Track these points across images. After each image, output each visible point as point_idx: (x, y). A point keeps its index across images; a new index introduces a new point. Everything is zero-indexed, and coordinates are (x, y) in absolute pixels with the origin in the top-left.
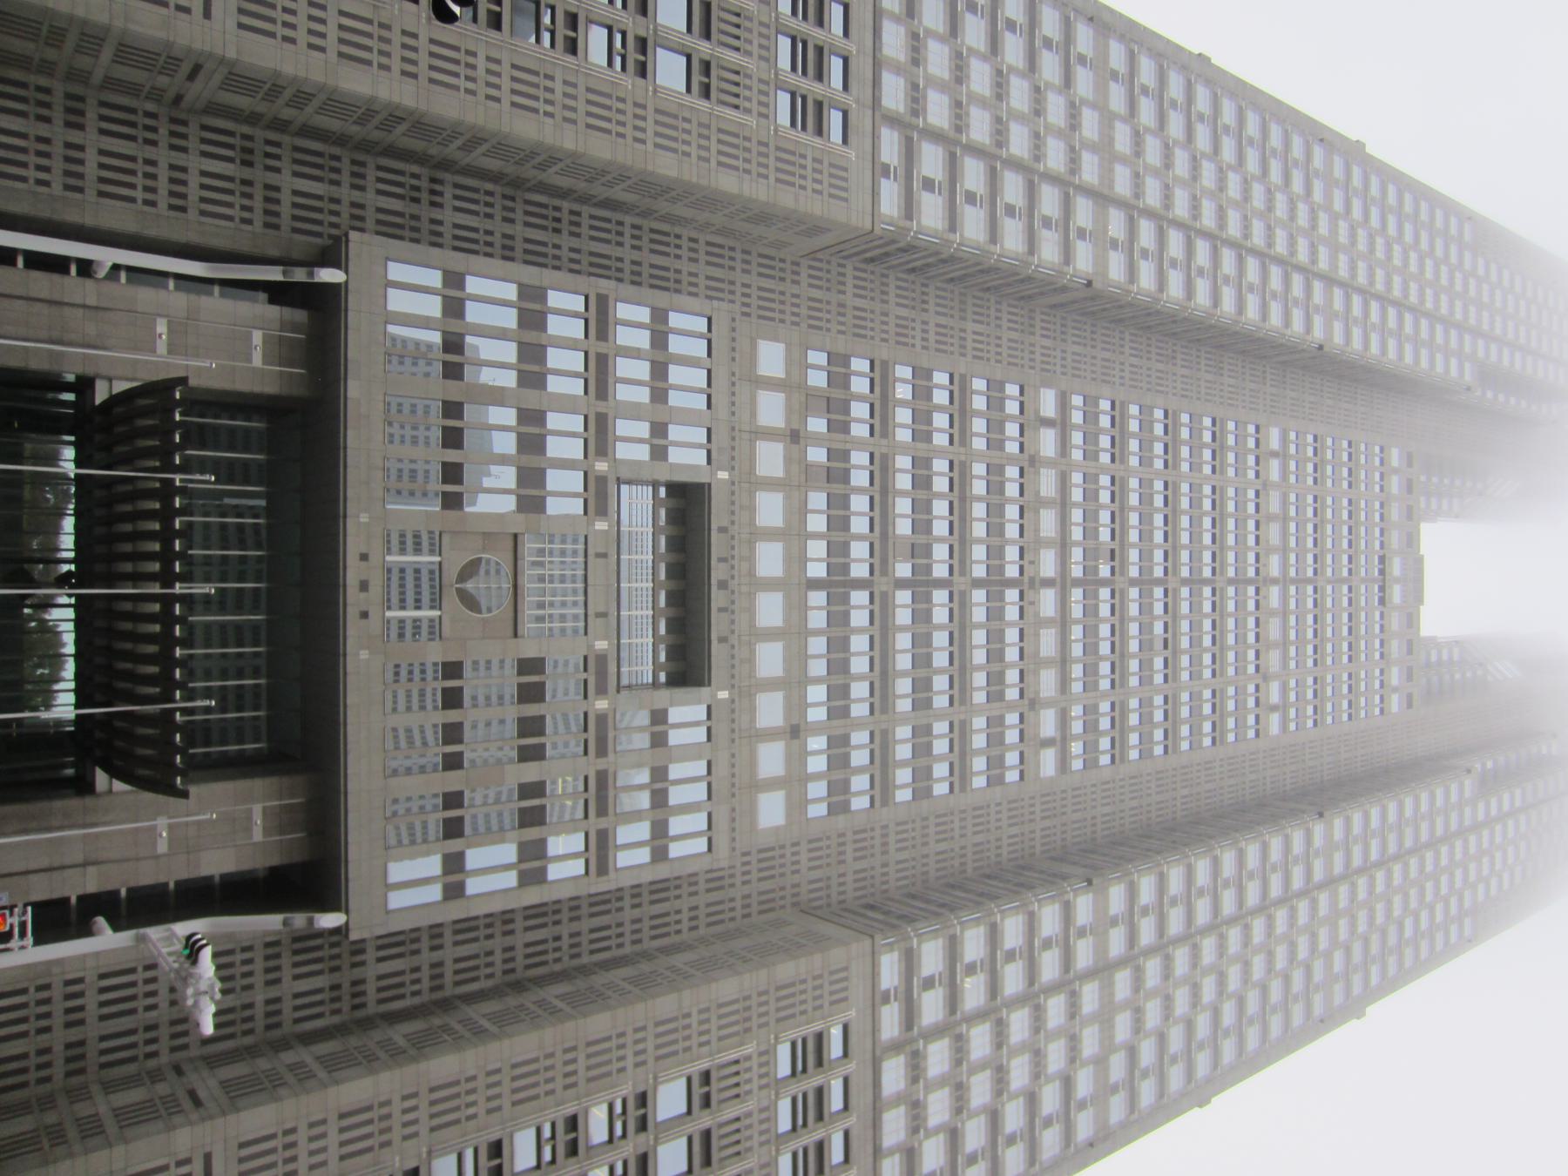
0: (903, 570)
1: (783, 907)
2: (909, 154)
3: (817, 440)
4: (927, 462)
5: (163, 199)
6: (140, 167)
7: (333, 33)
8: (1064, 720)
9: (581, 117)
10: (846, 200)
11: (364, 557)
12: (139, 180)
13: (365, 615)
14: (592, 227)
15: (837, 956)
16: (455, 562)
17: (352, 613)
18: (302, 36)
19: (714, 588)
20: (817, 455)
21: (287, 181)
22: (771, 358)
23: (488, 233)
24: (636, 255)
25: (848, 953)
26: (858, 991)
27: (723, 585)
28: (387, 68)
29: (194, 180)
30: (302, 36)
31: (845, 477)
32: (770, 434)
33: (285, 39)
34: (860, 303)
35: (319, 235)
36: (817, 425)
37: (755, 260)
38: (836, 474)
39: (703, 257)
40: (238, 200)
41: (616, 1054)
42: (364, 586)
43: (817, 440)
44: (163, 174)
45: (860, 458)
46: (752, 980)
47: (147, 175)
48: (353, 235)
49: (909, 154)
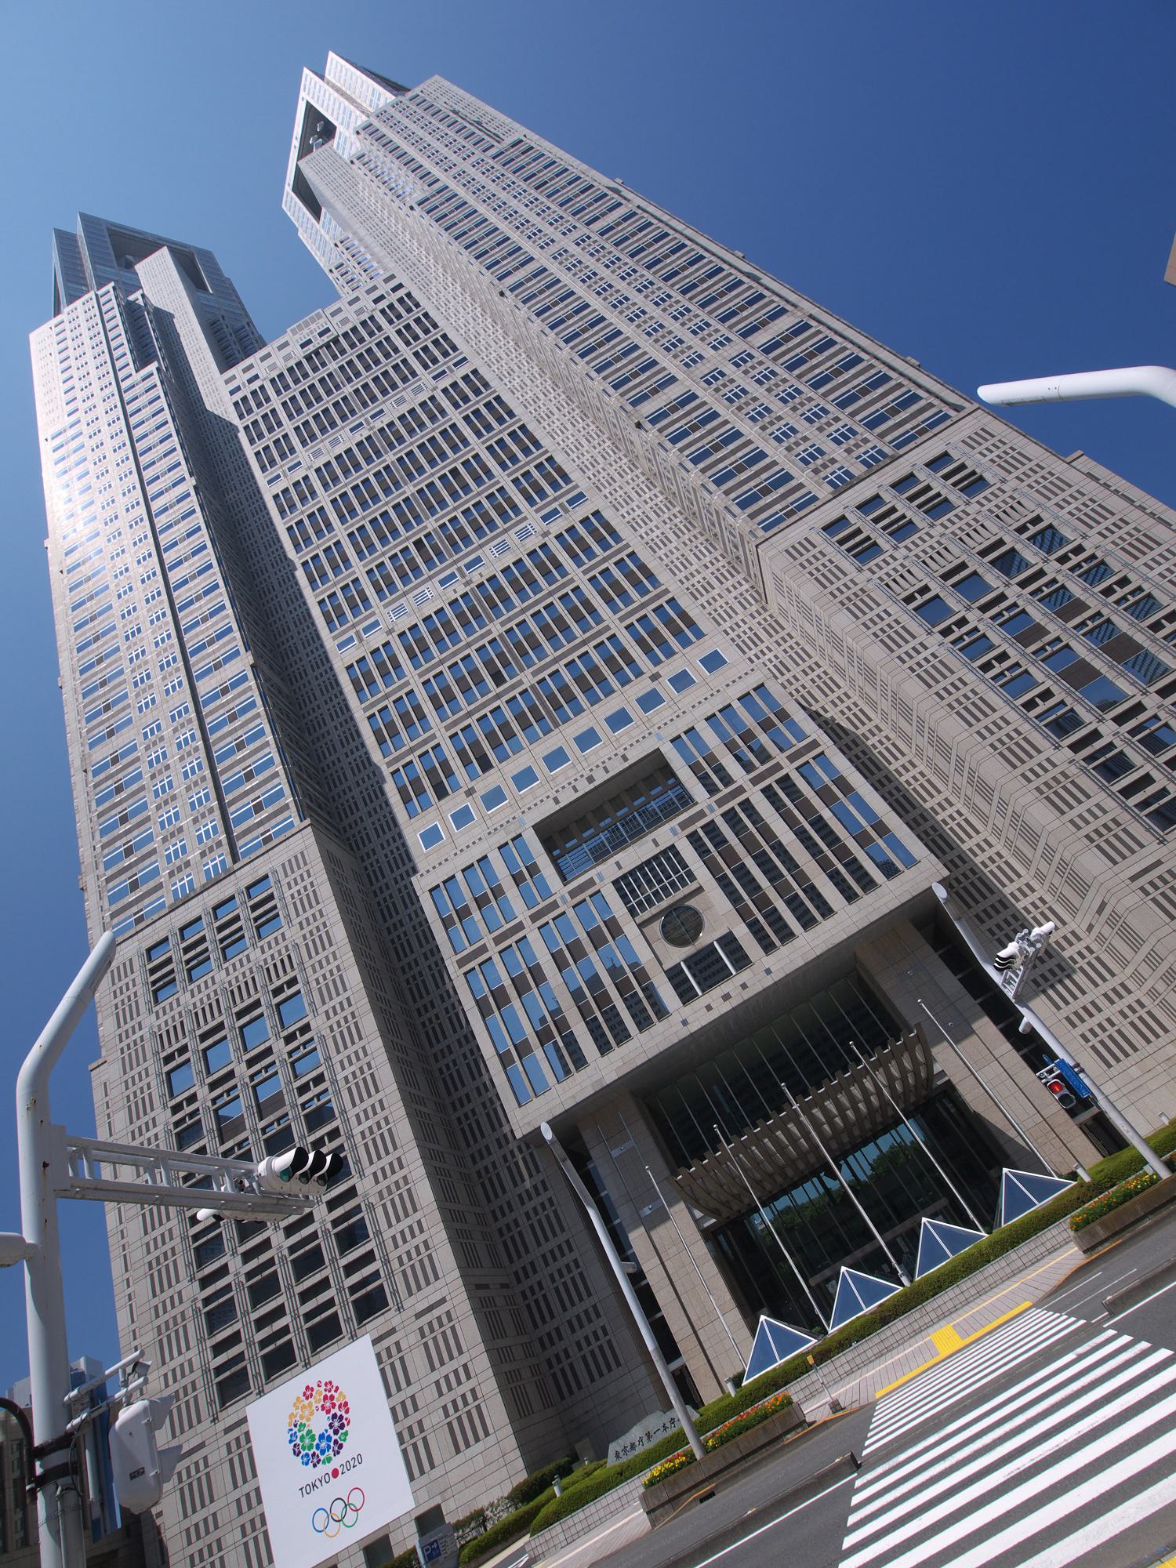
1: (771, 616)
5: (569, 1258)
6: (559, 1282)
7: (405, 1224)
9: (358, 1046)
10: (302, 853)
11: (709, 1008)
12: (567, 1278)
13: (744, 986)
14: (421, 997)
16: (676, 955)
17: (747, 994)
18: (419, 1239)
19: (596, 783)
23: (465, 1057)
24: (421, 960)
27: (590, 779)
28: (405, 1178)
29: (546, 1247)
30: (419, 1239)
33: (427, 1248)
34: (373, 836)
35: (531, 1155)
37: (376, 886)
39: (396, 919)
40: (542, 1216)
41: (926, 666)
42: (726, 997)
44: (553, 1268)
47: (561, 1276)
48: (518, 1135)
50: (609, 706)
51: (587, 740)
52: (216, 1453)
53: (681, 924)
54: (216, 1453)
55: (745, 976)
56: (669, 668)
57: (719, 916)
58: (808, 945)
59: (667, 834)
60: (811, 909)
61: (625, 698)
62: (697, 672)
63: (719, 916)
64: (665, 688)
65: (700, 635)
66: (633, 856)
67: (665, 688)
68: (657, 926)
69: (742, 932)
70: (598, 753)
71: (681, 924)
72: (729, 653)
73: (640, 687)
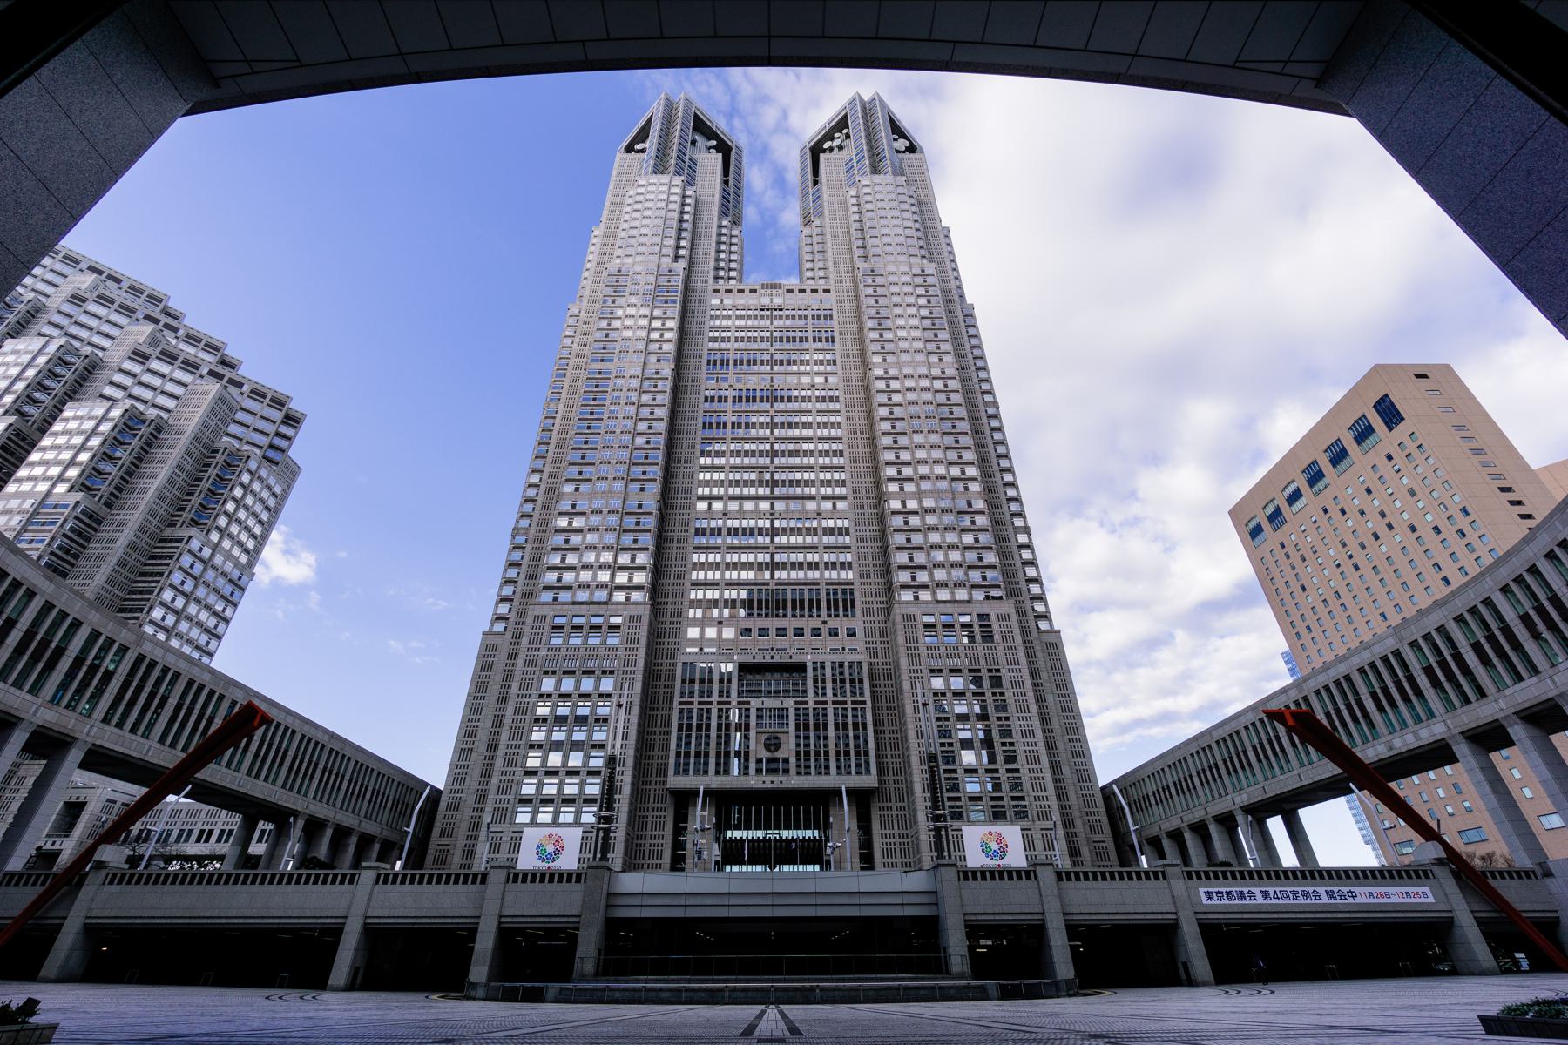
0: (767, 575)
2: (620, 588)
3: (721, 613)
4: (727, 565)
8: (825, 498)
15: (899, 619)
16: (764, 754)
20: (726, 612)
21: (651, 805)
22: (693, 633)
25: (898, 612)
26: (912, 610)
31: (734, 601)
32: (720, 633)
36: (716, 612)
38: (732, 604)
43: (721, 613)
45: (727, 594)
46: (902, 652)
49: (620, 588)
50: (799, 623)
51: (781, 632)
52: (506, 838)
53: (773, 743)
54: (506, 838)
55: (784, 779)
56: (832, 623)
57: (788, 748)
58: (814, 781)
59: (790, 702)
60: (824, 769)
61: (808, 624)
62: (843, 633)
63: (788, 748)
64: (825, 631)
65: (854, 615)
66: (771, 703)
67: (825, 631)
68: (764, 737)
69: (793, 760)
70: (781, 642)
71: (773, 743)
72: (860, 633)
73: (816, 623)
